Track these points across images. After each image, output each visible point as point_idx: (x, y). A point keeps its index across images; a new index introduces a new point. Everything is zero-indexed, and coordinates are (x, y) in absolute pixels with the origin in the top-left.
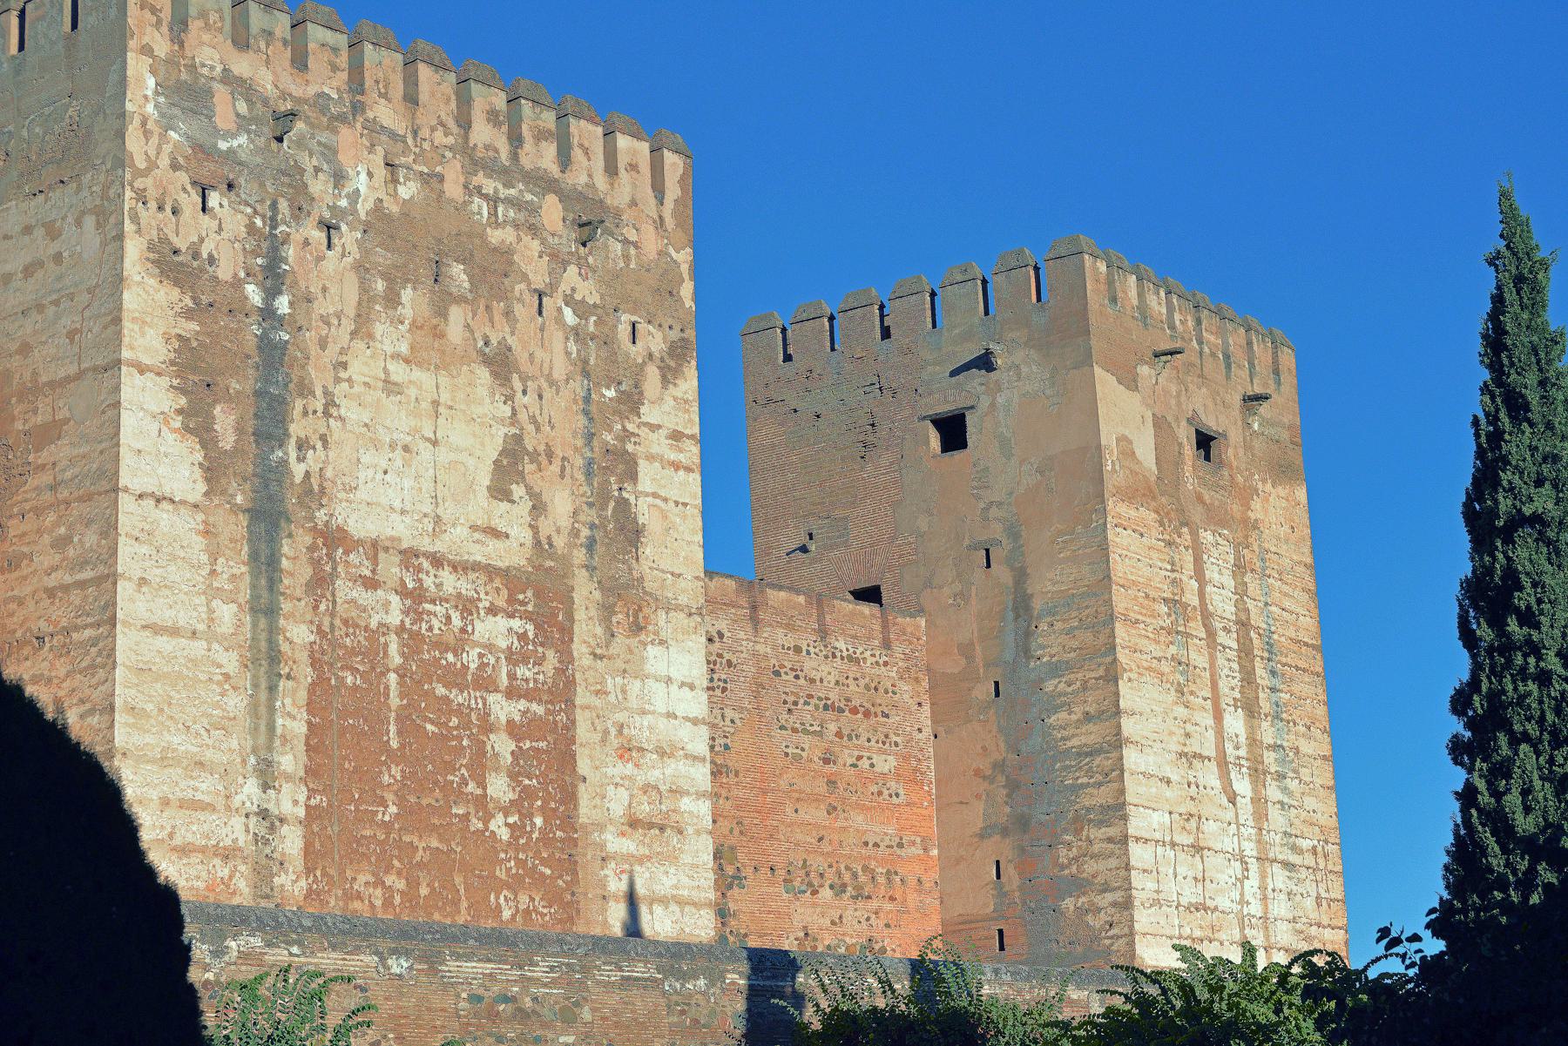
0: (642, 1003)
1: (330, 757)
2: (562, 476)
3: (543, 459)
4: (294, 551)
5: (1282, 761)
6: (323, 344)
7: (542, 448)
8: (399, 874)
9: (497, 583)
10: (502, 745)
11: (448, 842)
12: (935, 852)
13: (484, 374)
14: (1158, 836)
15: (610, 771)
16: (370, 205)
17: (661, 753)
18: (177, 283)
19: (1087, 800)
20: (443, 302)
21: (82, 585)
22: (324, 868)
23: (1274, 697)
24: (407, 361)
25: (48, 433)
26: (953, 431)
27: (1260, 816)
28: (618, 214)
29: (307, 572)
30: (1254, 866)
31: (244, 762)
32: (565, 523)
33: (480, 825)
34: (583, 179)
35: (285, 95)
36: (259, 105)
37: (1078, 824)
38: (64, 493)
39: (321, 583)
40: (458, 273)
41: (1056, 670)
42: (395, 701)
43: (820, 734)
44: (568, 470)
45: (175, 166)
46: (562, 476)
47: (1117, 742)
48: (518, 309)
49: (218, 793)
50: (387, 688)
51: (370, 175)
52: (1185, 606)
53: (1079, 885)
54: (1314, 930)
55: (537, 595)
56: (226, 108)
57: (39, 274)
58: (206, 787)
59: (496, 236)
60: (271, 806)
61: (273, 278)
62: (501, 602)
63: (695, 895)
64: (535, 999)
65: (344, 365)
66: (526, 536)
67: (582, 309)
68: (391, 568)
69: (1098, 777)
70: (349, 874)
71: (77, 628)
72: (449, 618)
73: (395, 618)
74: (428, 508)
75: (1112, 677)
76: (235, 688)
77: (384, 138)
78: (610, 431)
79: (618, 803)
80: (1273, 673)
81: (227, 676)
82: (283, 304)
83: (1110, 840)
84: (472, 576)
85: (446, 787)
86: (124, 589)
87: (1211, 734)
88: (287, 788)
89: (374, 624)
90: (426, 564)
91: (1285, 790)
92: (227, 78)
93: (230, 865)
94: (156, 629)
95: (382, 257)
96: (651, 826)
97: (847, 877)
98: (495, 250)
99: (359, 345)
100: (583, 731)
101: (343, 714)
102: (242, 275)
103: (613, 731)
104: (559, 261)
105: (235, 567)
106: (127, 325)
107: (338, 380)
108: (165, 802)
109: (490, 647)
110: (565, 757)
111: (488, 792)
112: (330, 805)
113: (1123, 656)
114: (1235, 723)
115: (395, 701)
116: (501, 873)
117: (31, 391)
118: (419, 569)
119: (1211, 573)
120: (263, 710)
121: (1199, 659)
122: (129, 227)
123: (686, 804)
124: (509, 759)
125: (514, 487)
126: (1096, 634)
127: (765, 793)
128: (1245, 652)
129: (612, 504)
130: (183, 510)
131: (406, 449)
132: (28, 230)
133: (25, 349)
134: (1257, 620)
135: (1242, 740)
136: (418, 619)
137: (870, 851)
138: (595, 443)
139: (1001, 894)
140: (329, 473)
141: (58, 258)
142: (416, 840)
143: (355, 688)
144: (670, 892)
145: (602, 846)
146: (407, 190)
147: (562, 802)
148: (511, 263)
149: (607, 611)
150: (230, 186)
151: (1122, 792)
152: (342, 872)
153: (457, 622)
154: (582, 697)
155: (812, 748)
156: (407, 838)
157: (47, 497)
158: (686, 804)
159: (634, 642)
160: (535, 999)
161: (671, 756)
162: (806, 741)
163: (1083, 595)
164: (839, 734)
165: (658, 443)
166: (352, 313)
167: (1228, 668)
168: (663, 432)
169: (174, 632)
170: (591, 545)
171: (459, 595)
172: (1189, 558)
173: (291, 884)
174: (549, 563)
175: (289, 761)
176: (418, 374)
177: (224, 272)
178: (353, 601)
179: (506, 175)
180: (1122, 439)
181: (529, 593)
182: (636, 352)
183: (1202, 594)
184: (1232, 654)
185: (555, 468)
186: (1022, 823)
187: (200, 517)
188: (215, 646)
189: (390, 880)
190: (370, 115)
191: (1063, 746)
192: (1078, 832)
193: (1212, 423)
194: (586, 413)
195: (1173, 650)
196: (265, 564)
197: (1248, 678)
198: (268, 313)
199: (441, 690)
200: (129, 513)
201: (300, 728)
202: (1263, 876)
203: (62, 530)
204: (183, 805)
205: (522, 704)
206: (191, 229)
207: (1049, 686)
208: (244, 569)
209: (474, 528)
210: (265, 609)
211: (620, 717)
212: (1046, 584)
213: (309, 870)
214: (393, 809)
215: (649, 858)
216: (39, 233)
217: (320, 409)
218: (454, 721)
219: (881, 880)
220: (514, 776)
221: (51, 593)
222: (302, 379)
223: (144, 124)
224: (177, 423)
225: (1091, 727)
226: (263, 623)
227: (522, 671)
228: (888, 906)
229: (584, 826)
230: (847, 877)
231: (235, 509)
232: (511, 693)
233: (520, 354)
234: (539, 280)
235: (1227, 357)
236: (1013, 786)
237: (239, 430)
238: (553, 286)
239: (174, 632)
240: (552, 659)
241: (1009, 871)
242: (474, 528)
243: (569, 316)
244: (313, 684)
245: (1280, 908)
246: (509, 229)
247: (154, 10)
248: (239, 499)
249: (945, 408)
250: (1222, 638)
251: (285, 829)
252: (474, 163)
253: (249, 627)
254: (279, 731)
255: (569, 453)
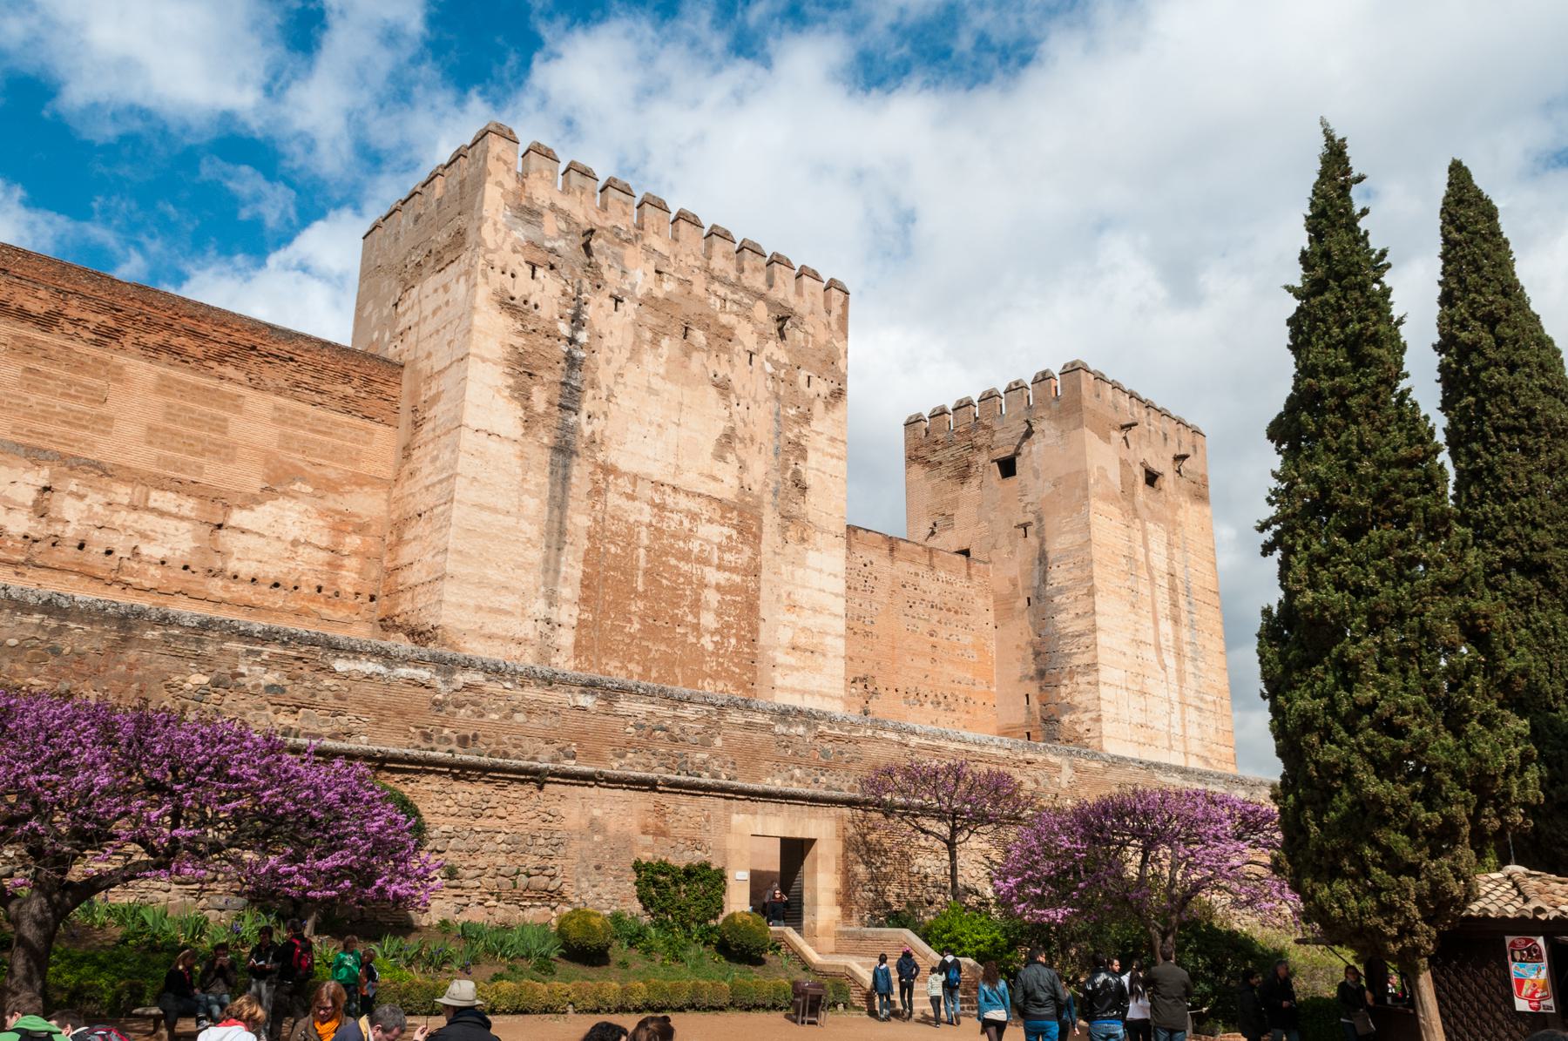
0: (757, 736)
1: (597, 592)
2: (760, 452)
3: (748, 441)
4: (580, 472)
5: (1195, 652)
6: (608, 362)
7: (747, 436)
8: (638, 663)
9: (714, 505)
10: (712, 597)
11: (673, 648)
12: (994, 689)
13: (713, 393)
14: (1118, 683)
15: (781, 617)
16: (644, 290)
17: (814, 610)
18: (513, 315)
19: (1076, 661)
20: (688, 350)
21: (440, 482)
22: (587, 657)
23: (1190, 616)
24: (663, 378)
25: (435, 400)
26: (1008, 467)
27: (1181, 678)
28: (801, 318)
29: (589, 487)
30: (1177, 707)
31: (537, 590)
32: (760, 476)
33: (694, 641)
34: (781, 296)
35: (590, 223)
36: (574, 226)
37: (1072, 673)
38: (438, 432)
39: (597, 492)
40: (698, 336)
41: (1060, 591)
42: (642, 563)
43: (928, 621)
44: (763, 450)
45: (515, 251)
46: (760, 452)
47: (1094, 629)
48: (736, 359)
49: (517, 606)
50: (638, 557)
51: (645, 274)
52: (1137, 561)
53: (1071, 708)
54: (1214, 746)
55: (740, 515)
56: (551, 225)
57: (439, 313)
58: (508, 601)
59: (724, 319)
60: (554, 618)
61: (577, 321)
62: (717, 517)
63: (832, 692)
64: (683, 729)
65: (622, 375)
66: (736, 483)
67: (776, 364)
68: (646, 491)
69: (1083, 649)
70: (604, 661)
71: (436, 506)
72: (681, 522)
73: (646, 519)
74: (672, 460)
75: (1091, 593)
76: (534, 546)
77: (655, 256)
78: (791, 430)
79: (785, 635)
80: (1190, 603)
81: (529, 540)
82: (582, 337)
83: (1089, 683)
84: (699, 500)
85: (673, 617)
86: (460, 483)
87: (1151, 632)
88: (565, 607)
89: (631, 520)
90: (668, 490)
91: (1196, 667)
92: (553, 208)
93: (522, 648)
94: (481, 507)
95: (651, 320)
96: (806, 650)
97: (941, 699)
98: (723, 326)
99: (632, 366)
100: (764, 594)
101: (609, 568)
102: (557, 317)
103: (784, 596)
104: (763, 337)
105: (540, 479)
106: (475, 335)
107: (616, 383)
108: (479, 608)
109: (708, 541)
110: (752, 607)
111: (702, 621)
112: (594, 620)
113: (1096, 582)
114: (1166, 627)
115: (642, 563)
116: (706, 668)
117: (430, 377)
118: (664, 493)
119: (1153, 545)
120: (552, 561)
121: (1144, 589)
122: (480, 279)
123: (829, 640)
124: (716, 604)
125: (728, 455)
126: (1082, 571)
127: (894, 648)
128: (1173, 589)
129: (790, 472)
130: (506, 442)
131: (659, 426)
132: (436, 291)
133: (429, 355)
134: (1180, 572)
135: (1171, 637)
136: (662, 519)
137: (956, 685)
138: (782, 436)
139: (1029, 712)
140: (607, 433)
141: (447, 303)
142: (650, 644)
143: (616, 555)
144: (815, 689)
145: (774, 659)
146: (669, 286)
147: (749, 631)
148: (733, 334)
149: (784, 529)
150: (552, 267)
151: (1096, 657)
152: (599, 659)
153: (686, 524)
154: (765, 575)
155: (923, 627)
156: (644, 643)
157: (431, 435)
158: (829, 640)
159: (800, 548)
160: (683, 729)
161: (821, 612)
162: (921, 624)
163: (1076, 550)
164: (939, 622)
165: (822, 442)
166: (629, 345)
167: (1163, 597)
168: (825, 436)
169: (495, 510)
170: (776, 493)
171: (689, 511)
172: (1139, 536)
173: (564, 663)
174: (748, 499)
175: (569, 591)
176: (669, 386)
177: (544, 312)
178: (619, 506)
179: (734, 286)
180: (1100, 468)
181: (735, 513)
182: (811, 392)
183: (1147, 556)
184: (1166, 591)
185: (755, 448)
186: (1041, 674)
187: (518, 447)
188: (522, 521)
189: (631, 666)
190: (647, 242)
191: (1063, 632)
192: (1071, 679)
193: (1156, 466)
194: (778, 421)
195: (1128, 583)
196: (561, 480)
197: (1175, 605)
198: (572, 341)
199: (673, 561)
200: (467, 439)
201: (579, 575)
202: (1183, 712)
203: (435, 453)
204: (492, 610)
205: (727, 575)
206: (523, 286)
207: (1057, 600)
208: (547, 480)
209: (701, 474)
210: (559, 503)
211: (789, 588)
212: (1056, 546)
213: (576, 657)
214: (637, 626)
215: (803, 668)
216: (441, 291)
217: (604, 398)
218: (682, 580)
219: (962, 701)
220: (719, 615)
221: (427, 488)
222: (593, 380)
223: (495, 224)
224: (507, 393)
225: (1079, 621)
226: (556, 512)
227: (727, 556)
228: (967, 716)
229: (763, 647)
230: (941, 699)
231: (542, 446)
232: (719, 567)
233: (736, 384)
234: (752, 346)
235: (1165, 435)
236: (1037, 654)
237: (550, 403)
238: (759, 351)
239: (495, 510)
240: (748, 551)
241: (1033, 700)
242: (701, 474)
243: (769, 368)
244: (588, 550)
245: (1193, 731)
246: (733, 316)
247: (505, 163)
248: (546, 440)
249: (1004, 452)
250: (1159, 581)
251: (561, 631)
252: (713, 278)
253: (546, 513)
254: (562, 574)
255: (765, 441)
